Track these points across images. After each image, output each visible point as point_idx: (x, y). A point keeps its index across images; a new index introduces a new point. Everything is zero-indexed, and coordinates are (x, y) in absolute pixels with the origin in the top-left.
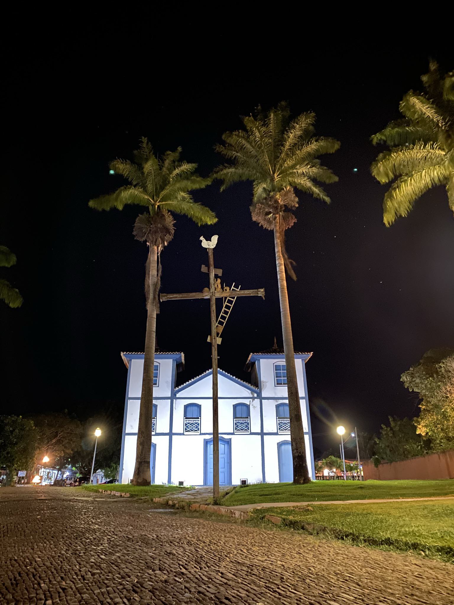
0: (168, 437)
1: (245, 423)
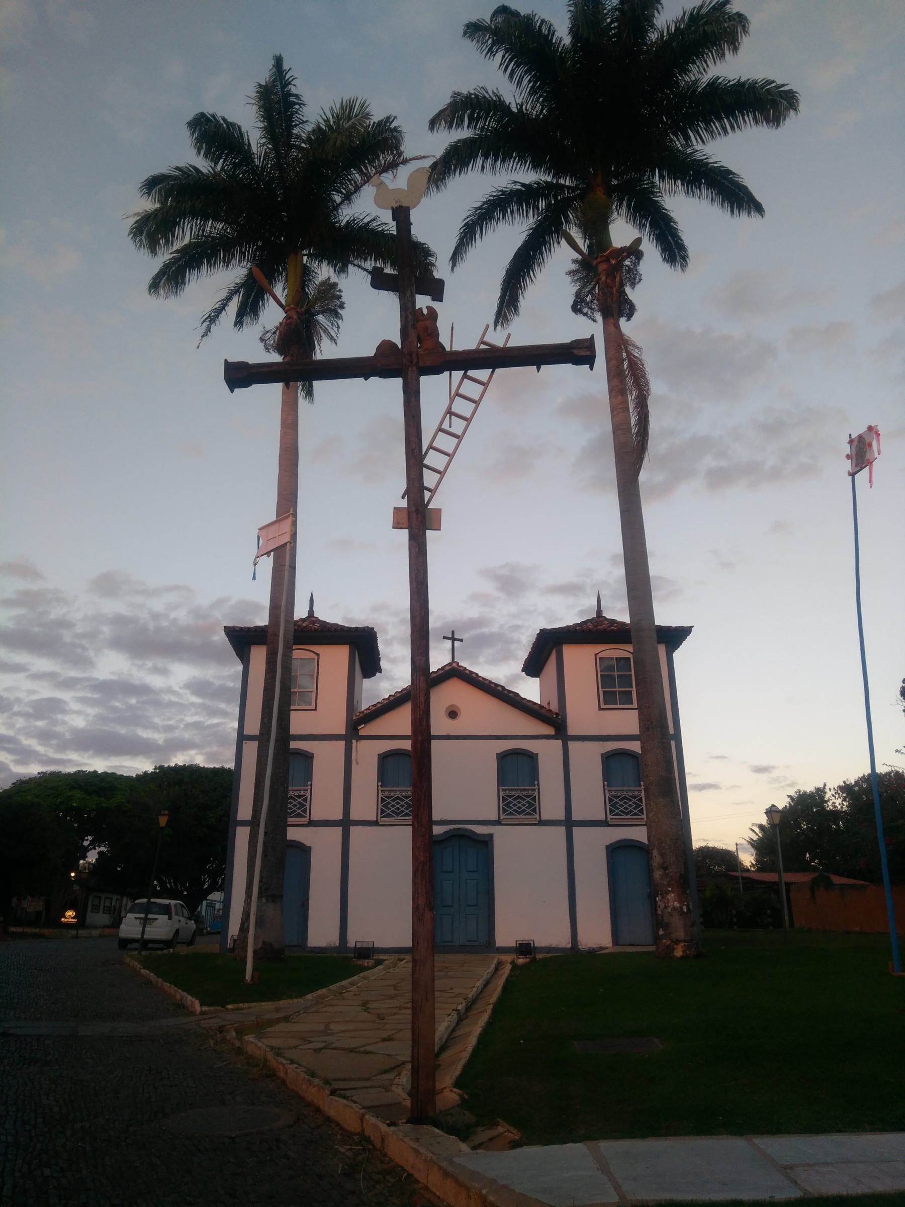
0: (338, 831)
1: (528, 796)
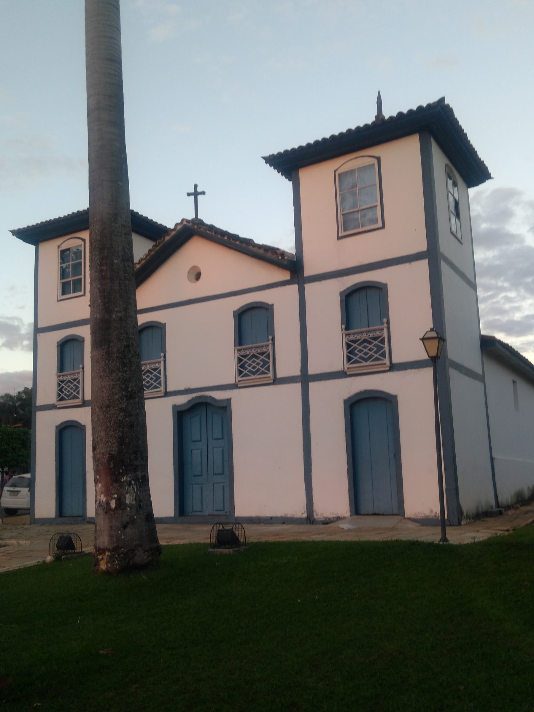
1: (262, 354)
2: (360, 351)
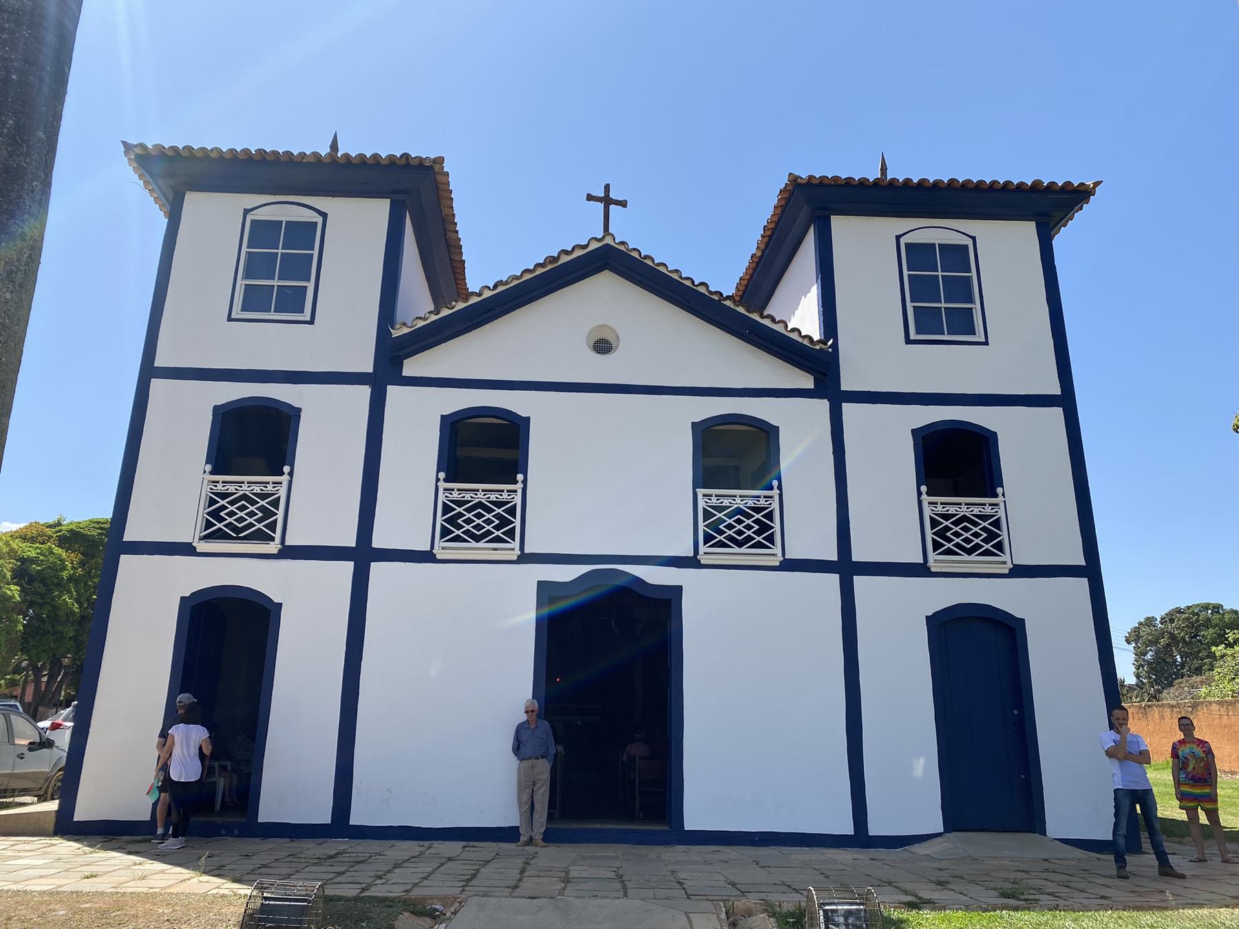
2: (957, 534)
